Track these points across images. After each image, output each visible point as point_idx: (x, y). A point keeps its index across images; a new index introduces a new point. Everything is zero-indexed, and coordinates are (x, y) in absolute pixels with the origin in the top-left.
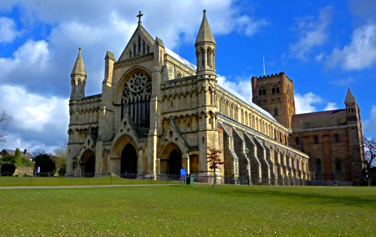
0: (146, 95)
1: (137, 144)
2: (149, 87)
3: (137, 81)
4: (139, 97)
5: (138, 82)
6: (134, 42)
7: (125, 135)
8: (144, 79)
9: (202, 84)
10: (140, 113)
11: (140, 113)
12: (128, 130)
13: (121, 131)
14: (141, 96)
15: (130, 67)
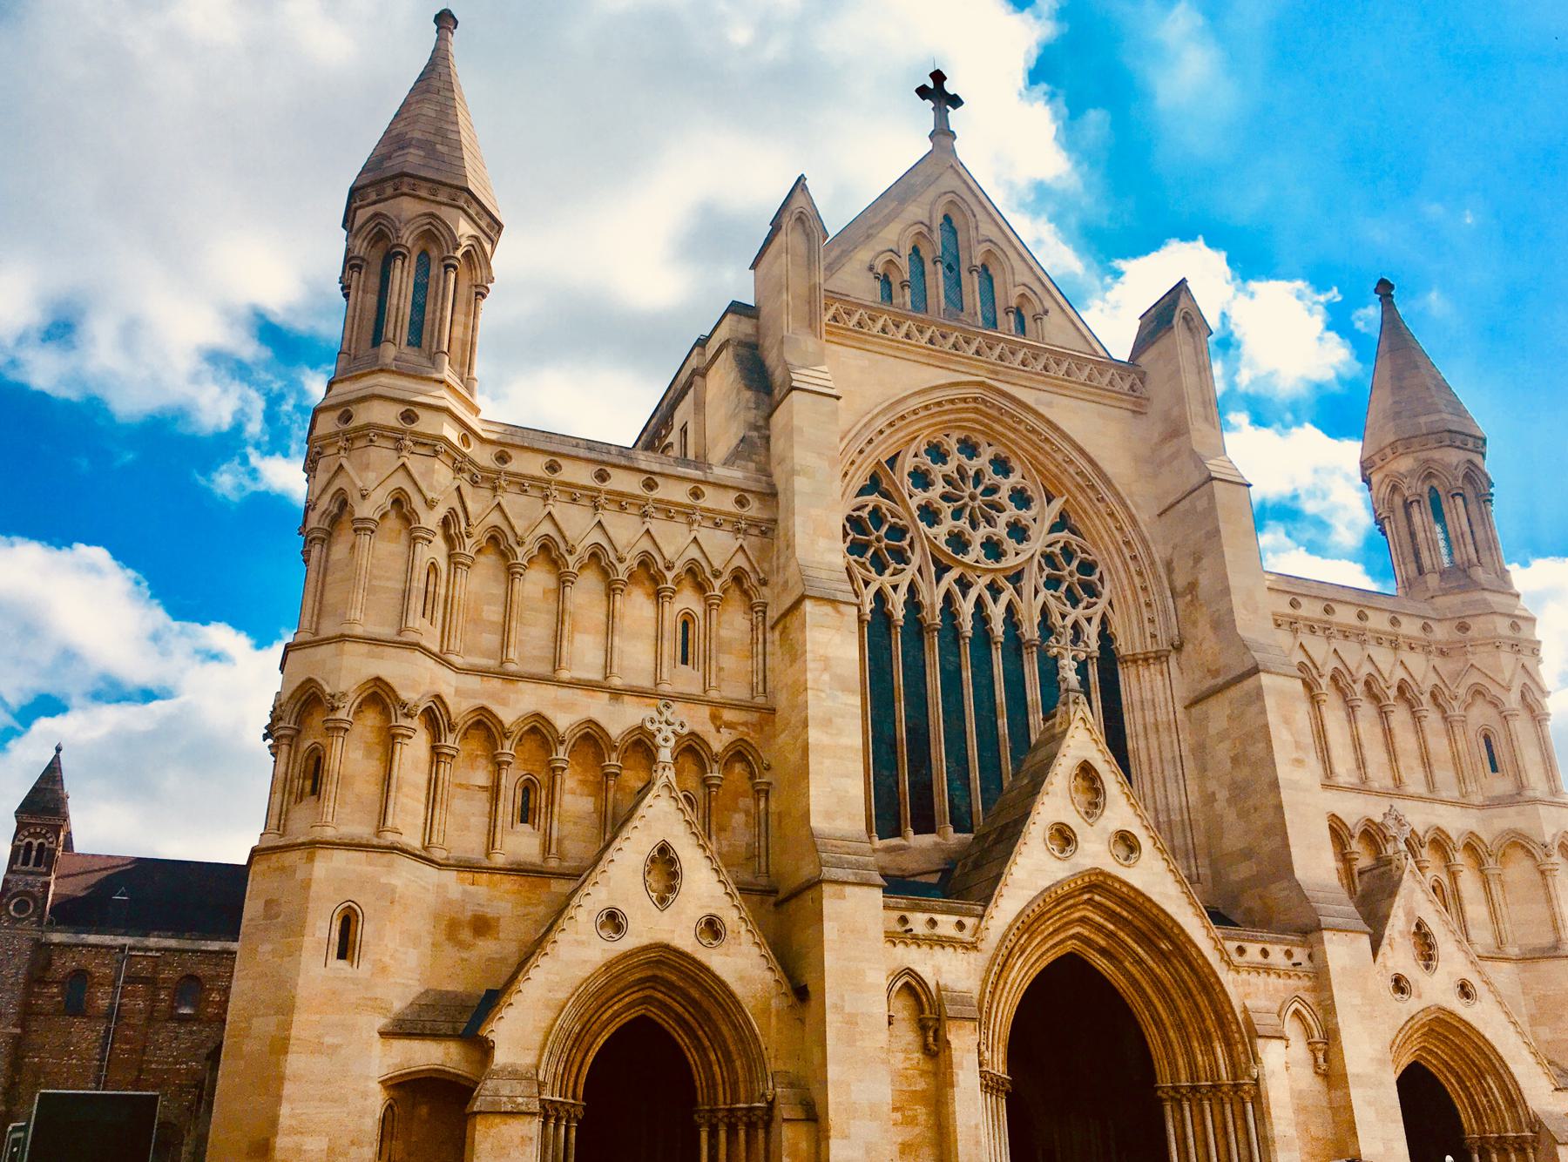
0: (1045, 611)
1: (1227, 977)
2: (1075, 563)
3: (981, 488)
4: (997, 612)
5: (973, 497)
6: (925, 230)
7: (1097, 884)
8: (1021, 498)
9: (1467, 660)
10: (1003, 723)
11: (1003, 723)
12: (1127, 842)
13: (1064, 837)
14: (1010, 609)
15: (943, 377)
